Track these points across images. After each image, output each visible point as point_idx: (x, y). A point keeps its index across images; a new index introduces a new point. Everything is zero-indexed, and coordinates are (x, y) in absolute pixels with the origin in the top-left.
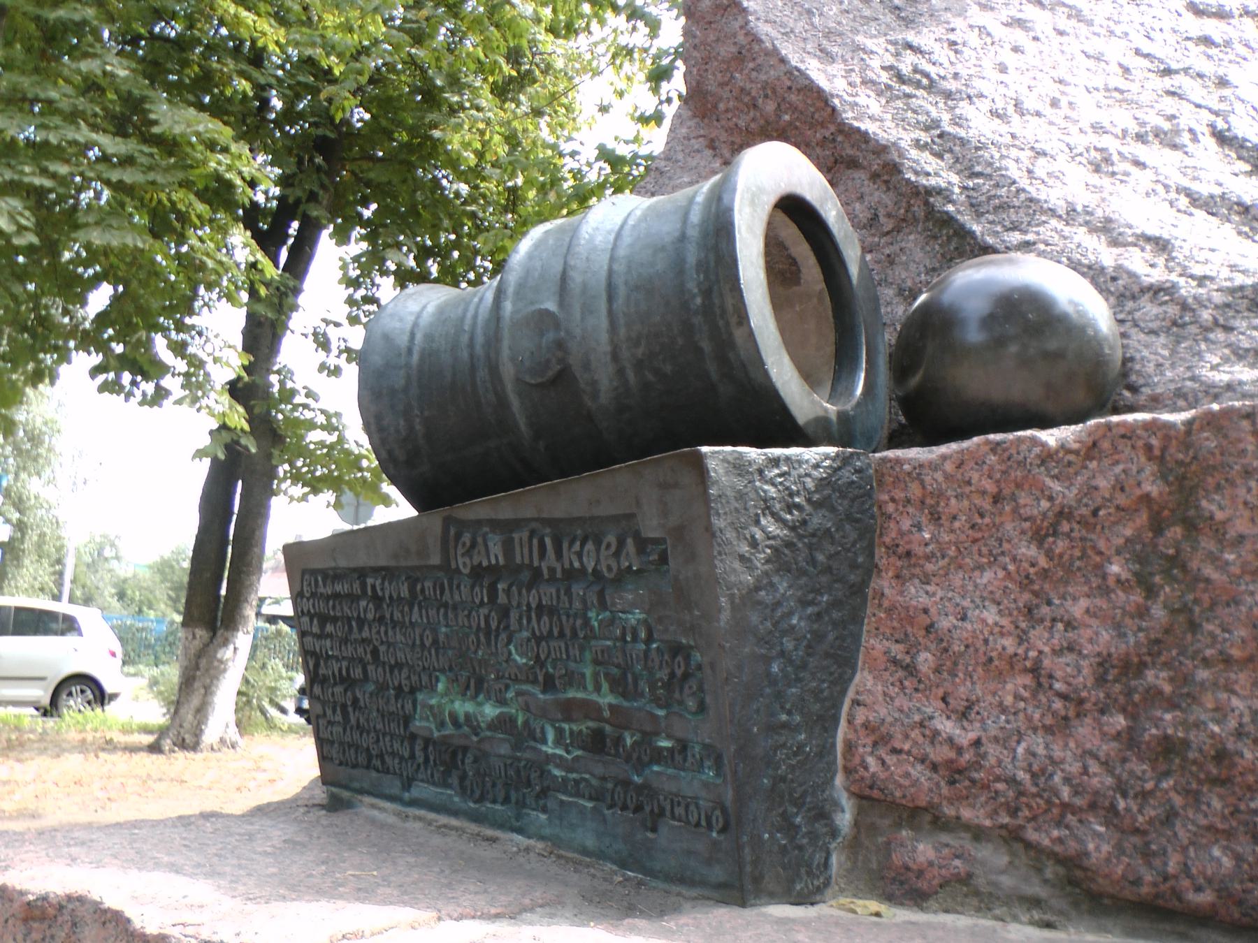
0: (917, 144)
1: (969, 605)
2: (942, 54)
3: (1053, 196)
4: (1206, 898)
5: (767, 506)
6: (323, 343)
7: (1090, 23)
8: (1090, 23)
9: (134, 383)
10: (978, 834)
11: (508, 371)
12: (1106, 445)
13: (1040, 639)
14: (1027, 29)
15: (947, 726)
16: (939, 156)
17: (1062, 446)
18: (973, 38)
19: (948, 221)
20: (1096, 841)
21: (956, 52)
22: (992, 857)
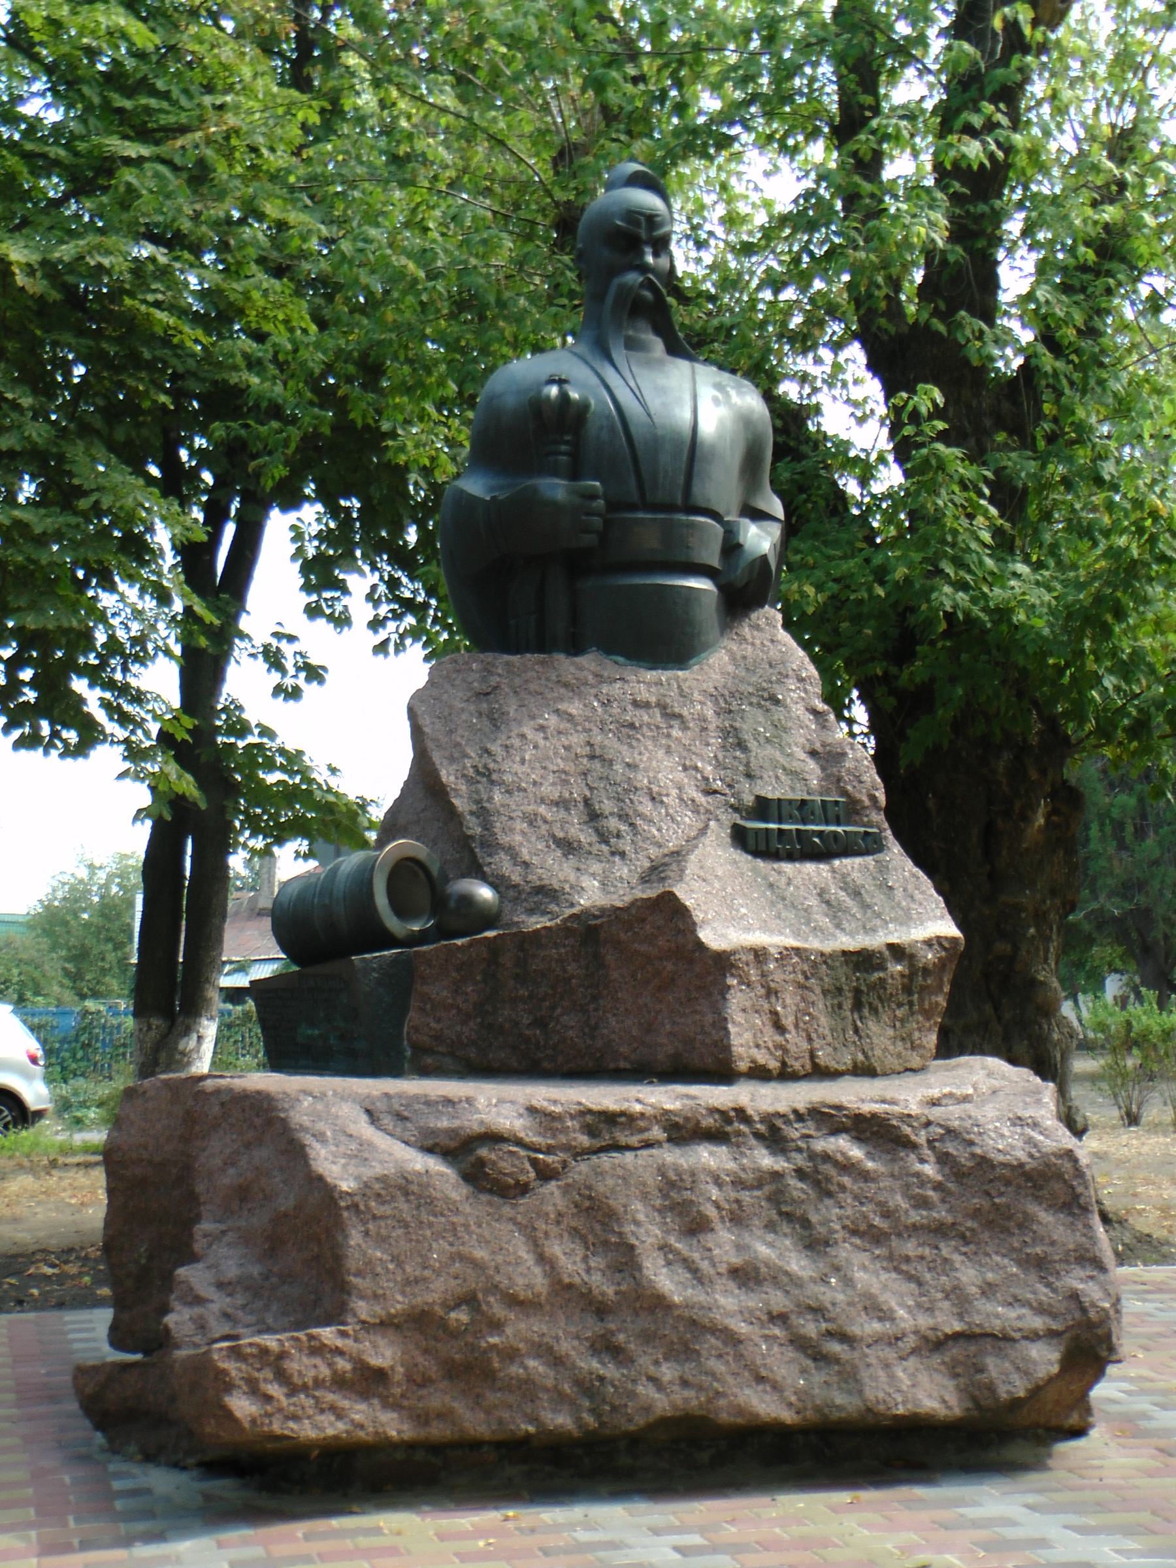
0: (472, 813)
1: (439, 991)
3: (504, 839)
4: (497, 1065)
5: (374, 970)
6: (273, 659)
9: (55, 734)
10: (443, 1054)
13: (459, 1000)
15: (433, 1025)
18: (516, 742)
19: (472, 851)
20: (472, 1053)
22: (448, 1061)
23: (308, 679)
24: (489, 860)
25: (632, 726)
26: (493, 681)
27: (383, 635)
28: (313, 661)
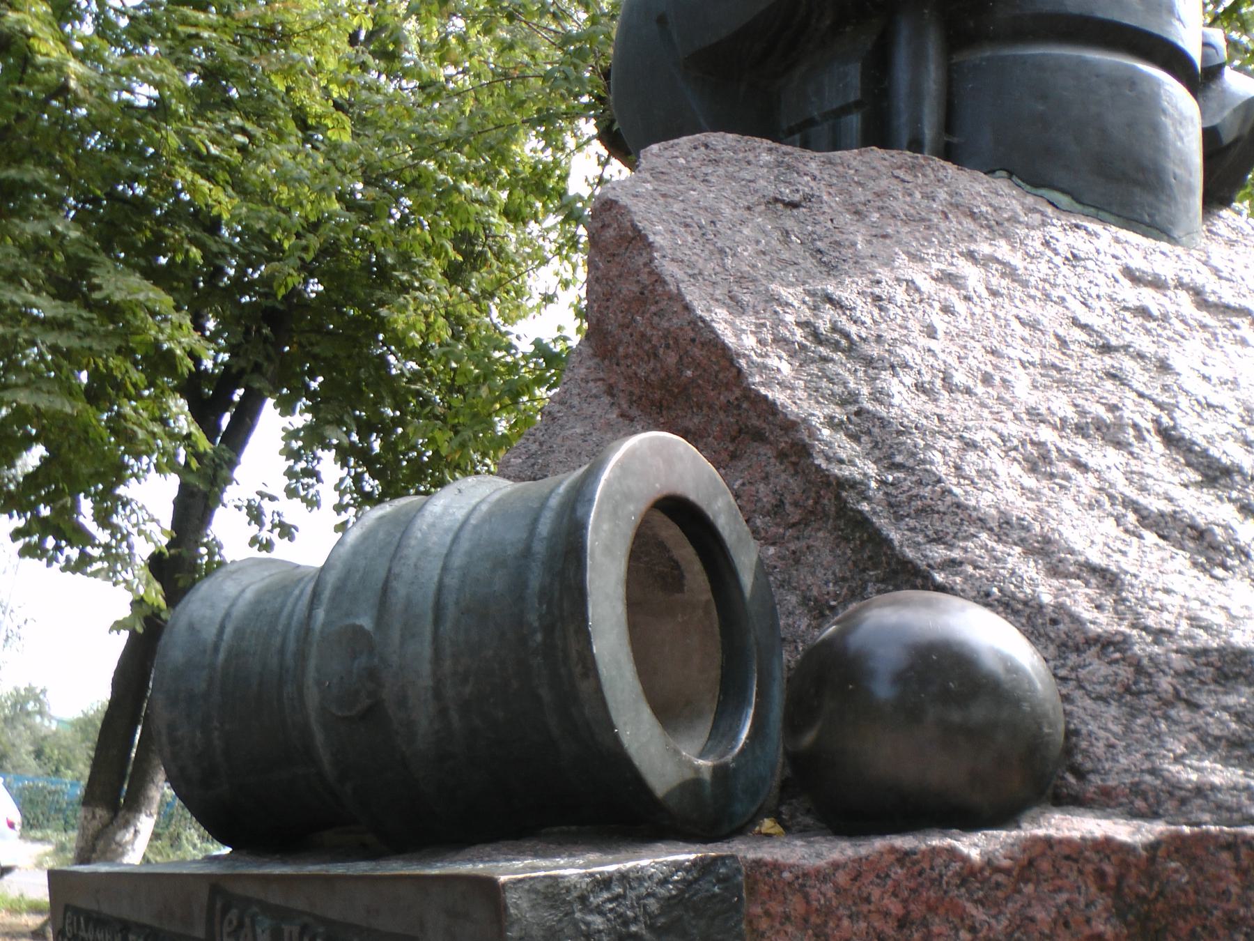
0: (831, 422)
2: (865, 311)
6: (255, 515)
7: (1025, 284)
8: (1025, 284)
9: (58, 548)
11: (313, 697)
12: (1045, 865)
14: (958, 287)
16: (855, 438)
17: (989, 862)
18: (900, 295)
19: (862, 522)
21: (881, 309)
23: (281, 536)
24: (939, 553)
25: (1143, 312)
26: (805, 184)
27: (344, 517)
28: (287, 520)
